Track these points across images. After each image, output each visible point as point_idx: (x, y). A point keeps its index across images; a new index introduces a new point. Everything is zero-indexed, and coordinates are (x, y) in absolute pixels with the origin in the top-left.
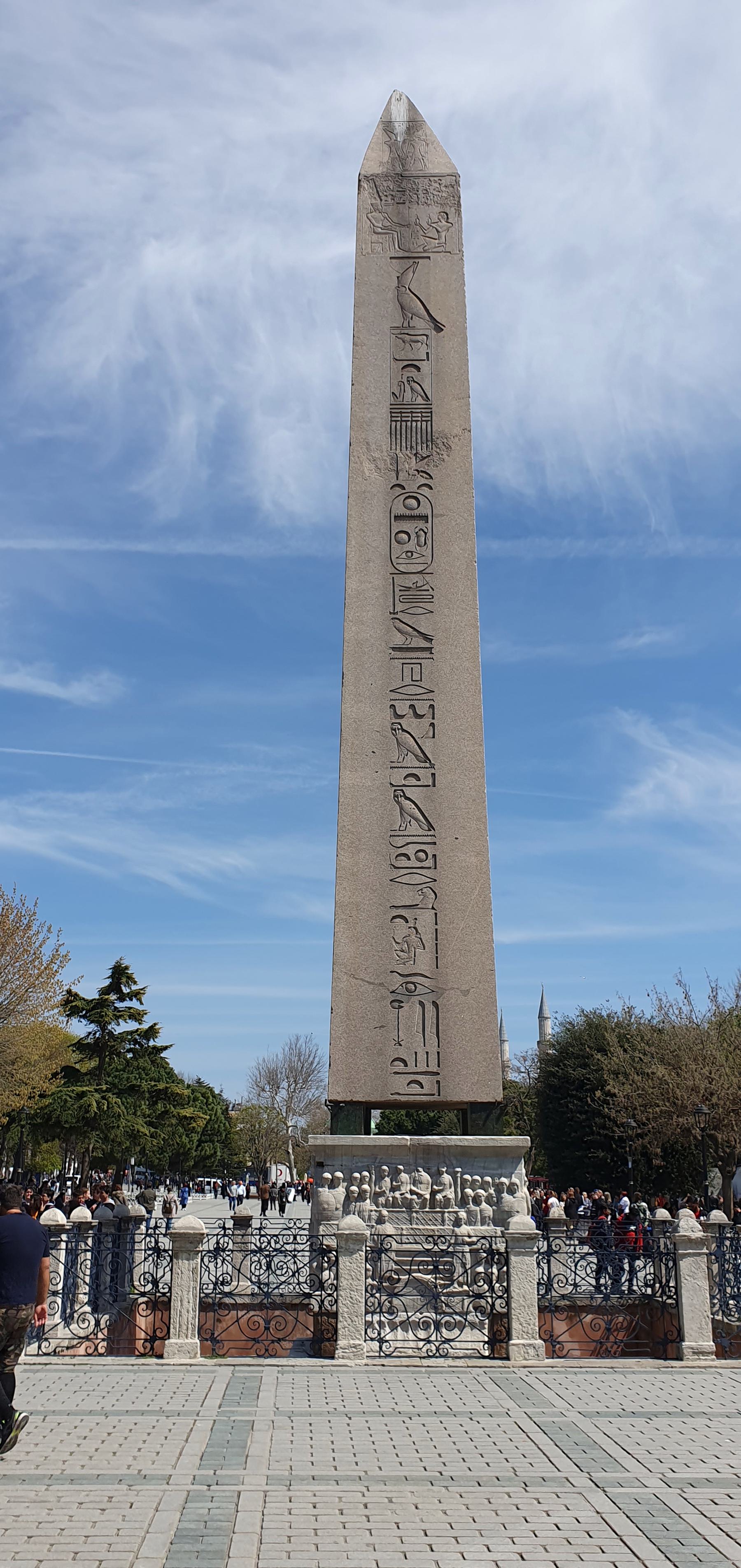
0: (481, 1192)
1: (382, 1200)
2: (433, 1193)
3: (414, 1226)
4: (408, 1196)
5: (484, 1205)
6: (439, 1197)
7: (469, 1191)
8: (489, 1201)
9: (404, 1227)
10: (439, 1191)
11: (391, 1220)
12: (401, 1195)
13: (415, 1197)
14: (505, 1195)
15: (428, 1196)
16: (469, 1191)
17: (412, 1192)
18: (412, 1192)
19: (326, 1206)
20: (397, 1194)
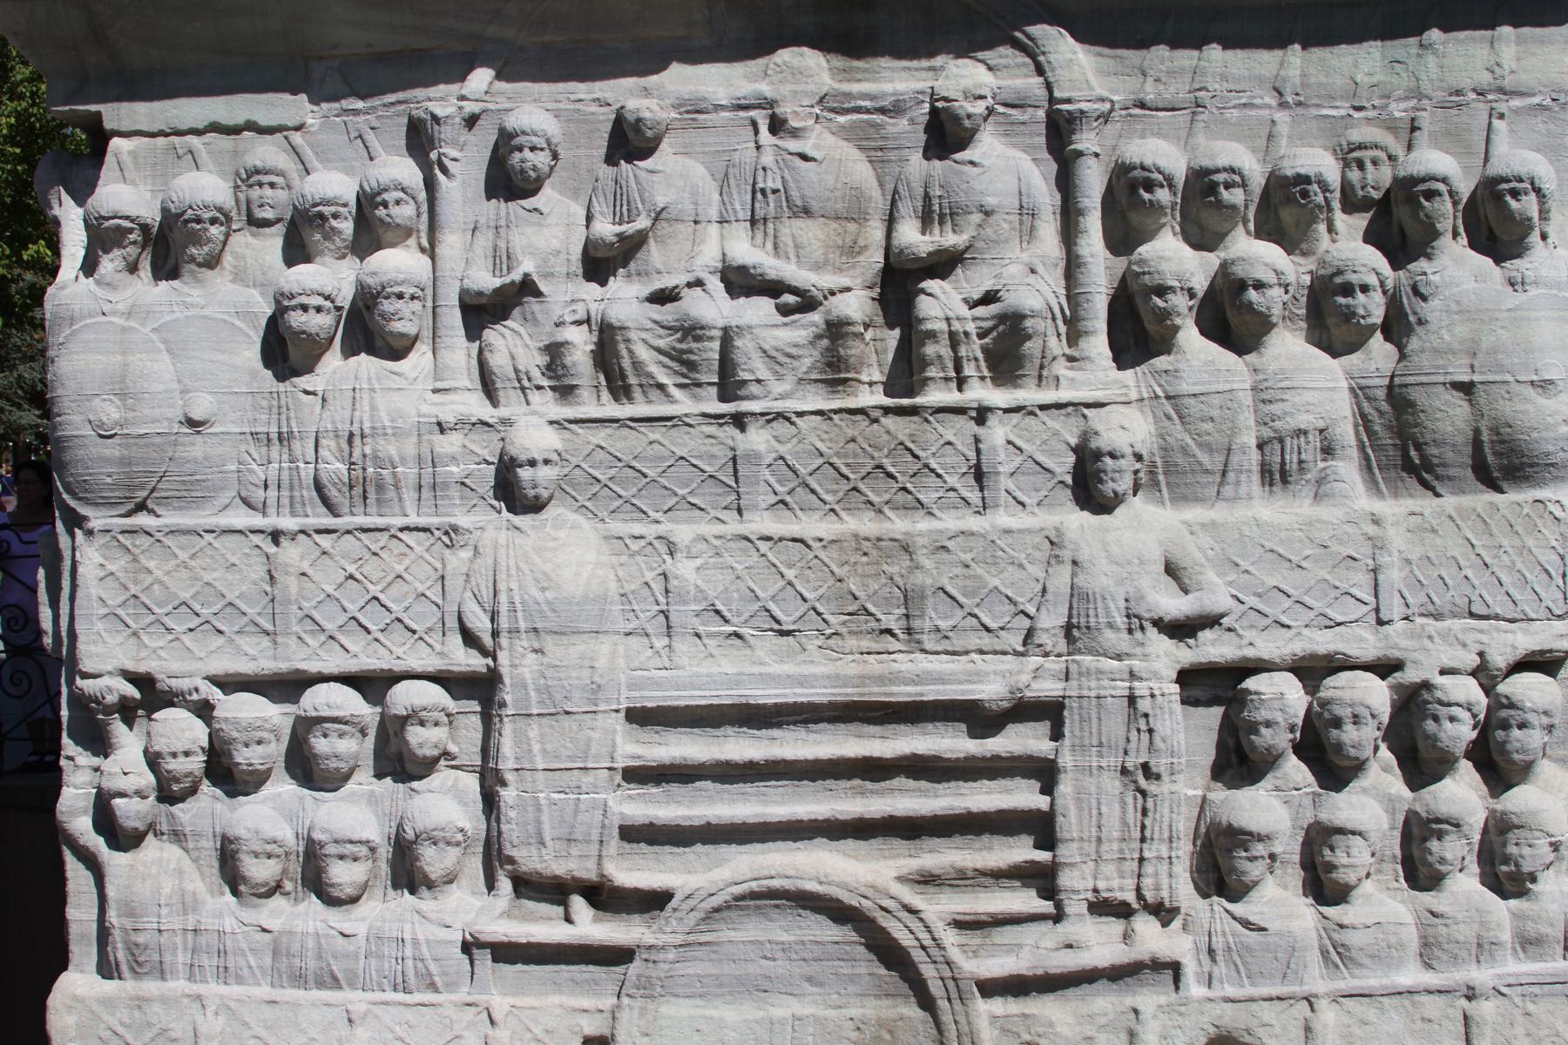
0: (1254, 253)
1: (512, 344)
2: (900, 283)
3: (762, 523)
4: (713, 307)
5: (1288, 347)
6: (941, 303)
7: (1172, 256)
8: (1329, 316)
9: (683, 532)
10: (944, 264)
11: (597, 491)
12: (663, 297)
13: (759, 310)
14: (1456, 266)
15: (856, 305)
16: (1172, 256)
17: (740, 281)
18: (740, 281)
19: (110, 412)
20: (623, 299)
